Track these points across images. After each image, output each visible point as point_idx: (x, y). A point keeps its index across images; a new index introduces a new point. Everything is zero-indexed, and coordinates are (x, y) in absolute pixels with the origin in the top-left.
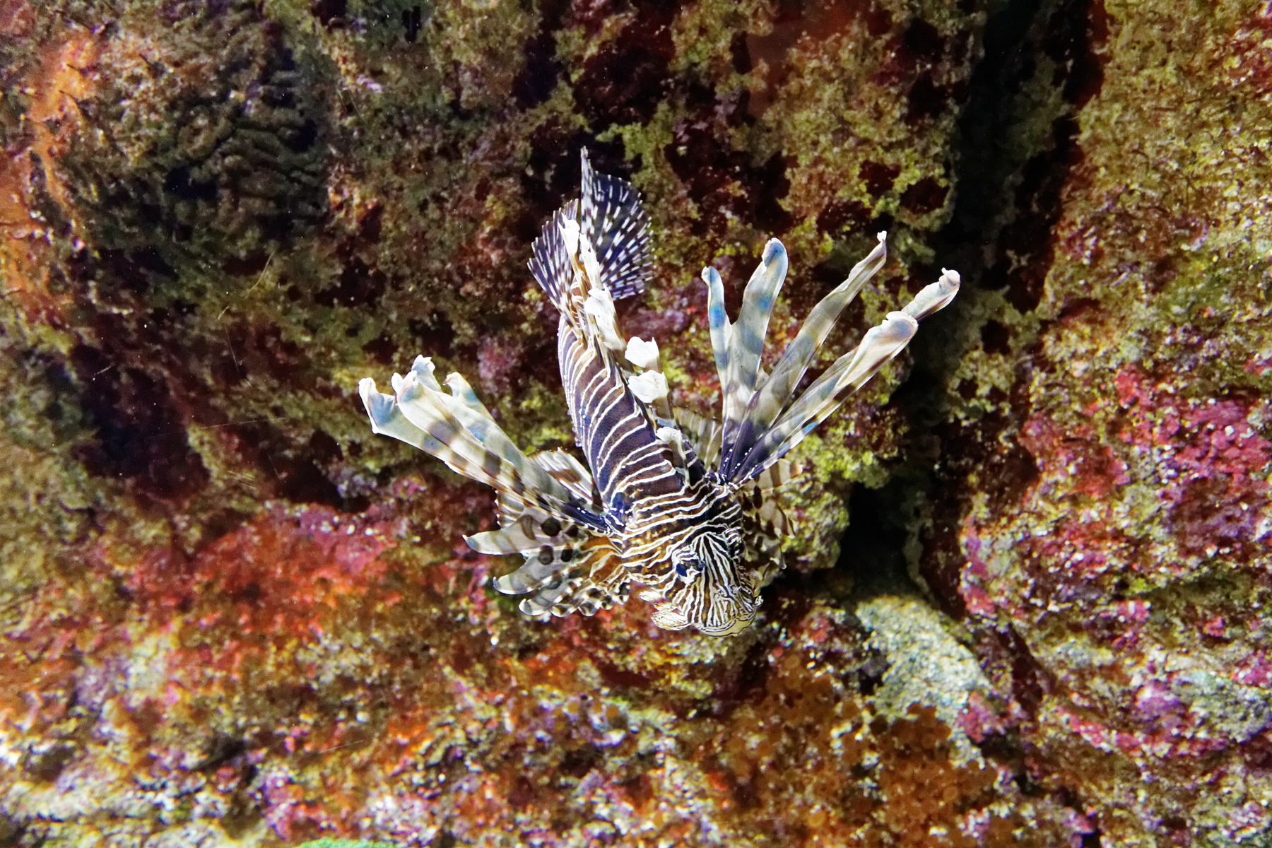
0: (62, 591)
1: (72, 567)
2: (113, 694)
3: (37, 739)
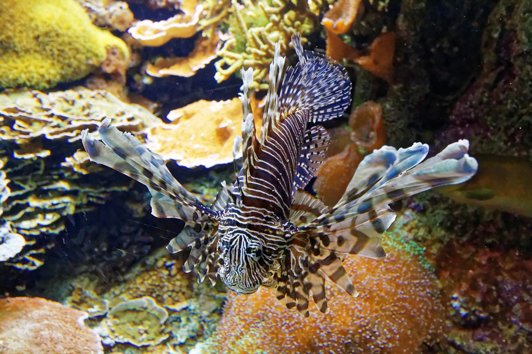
0: (500, 231)
2: (521, 300)
3: (481, 309)
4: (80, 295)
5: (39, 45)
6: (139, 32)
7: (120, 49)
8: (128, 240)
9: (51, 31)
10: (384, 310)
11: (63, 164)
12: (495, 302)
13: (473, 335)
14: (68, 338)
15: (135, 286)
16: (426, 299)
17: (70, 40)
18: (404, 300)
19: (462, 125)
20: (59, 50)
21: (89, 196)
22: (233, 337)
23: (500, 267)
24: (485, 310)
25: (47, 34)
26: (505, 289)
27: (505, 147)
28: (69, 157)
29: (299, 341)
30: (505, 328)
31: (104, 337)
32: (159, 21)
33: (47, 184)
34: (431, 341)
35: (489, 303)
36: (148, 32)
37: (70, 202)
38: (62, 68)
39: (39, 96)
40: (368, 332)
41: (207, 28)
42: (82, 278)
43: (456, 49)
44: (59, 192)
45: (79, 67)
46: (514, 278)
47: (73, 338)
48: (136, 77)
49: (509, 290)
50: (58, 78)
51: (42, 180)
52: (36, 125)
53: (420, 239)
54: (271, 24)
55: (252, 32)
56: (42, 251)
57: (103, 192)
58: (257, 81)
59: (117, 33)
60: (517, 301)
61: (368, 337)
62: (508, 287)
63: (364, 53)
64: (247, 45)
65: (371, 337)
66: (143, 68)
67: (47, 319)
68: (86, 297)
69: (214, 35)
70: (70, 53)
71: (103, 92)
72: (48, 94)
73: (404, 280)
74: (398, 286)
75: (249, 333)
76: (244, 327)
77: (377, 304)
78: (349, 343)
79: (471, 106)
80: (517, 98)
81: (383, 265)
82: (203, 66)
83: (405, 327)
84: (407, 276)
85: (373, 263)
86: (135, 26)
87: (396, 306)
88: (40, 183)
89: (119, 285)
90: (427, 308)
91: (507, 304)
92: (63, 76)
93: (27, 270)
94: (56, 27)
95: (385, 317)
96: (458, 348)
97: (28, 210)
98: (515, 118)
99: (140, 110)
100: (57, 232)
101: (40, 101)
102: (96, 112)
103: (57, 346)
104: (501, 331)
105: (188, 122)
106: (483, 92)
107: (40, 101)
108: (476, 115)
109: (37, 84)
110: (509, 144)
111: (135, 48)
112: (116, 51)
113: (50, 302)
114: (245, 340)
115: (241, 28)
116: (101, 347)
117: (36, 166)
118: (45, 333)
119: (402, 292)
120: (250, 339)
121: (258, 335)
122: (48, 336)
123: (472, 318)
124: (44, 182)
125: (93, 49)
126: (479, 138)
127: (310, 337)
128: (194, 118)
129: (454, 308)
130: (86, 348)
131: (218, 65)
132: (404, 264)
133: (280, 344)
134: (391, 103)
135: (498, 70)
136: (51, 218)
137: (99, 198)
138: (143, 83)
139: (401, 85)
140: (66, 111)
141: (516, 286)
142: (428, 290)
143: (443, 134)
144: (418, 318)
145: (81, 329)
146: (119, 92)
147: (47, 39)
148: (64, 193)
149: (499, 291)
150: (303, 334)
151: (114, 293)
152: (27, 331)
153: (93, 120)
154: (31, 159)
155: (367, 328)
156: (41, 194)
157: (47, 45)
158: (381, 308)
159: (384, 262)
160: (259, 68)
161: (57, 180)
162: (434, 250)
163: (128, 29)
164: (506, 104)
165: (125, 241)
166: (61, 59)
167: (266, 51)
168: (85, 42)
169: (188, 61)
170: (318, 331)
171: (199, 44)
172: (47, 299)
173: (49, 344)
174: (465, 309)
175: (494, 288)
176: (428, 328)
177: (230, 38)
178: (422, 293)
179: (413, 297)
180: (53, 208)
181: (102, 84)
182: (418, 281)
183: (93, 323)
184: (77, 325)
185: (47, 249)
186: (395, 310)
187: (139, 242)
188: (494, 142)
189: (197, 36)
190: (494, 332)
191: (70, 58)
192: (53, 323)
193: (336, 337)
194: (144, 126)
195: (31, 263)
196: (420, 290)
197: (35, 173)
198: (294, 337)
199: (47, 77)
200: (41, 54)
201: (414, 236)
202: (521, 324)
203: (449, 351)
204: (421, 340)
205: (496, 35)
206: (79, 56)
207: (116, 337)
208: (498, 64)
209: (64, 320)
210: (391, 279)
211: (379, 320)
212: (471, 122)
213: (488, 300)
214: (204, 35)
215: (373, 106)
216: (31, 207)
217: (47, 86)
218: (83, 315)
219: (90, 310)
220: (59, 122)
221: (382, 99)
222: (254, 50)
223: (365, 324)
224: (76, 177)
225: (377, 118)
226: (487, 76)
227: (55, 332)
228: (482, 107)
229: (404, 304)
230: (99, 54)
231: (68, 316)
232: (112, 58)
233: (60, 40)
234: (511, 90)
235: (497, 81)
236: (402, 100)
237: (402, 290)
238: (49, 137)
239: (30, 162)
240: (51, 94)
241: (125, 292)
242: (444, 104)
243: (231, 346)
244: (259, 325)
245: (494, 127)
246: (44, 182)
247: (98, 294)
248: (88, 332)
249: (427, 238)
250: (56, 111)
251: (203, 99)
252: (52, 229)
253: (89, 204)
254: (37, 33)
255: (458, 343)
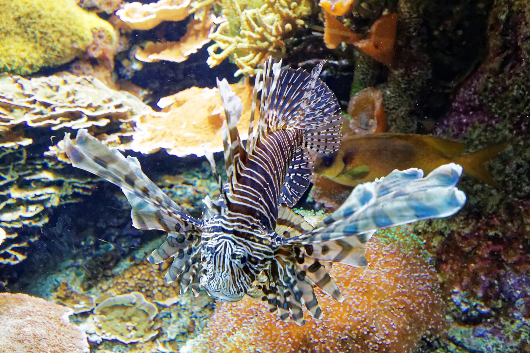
0: (504, 223)
1: (516, 211)
3: (483, 304)
4: (65, 290)
5: (20, 27)
6: (128, 15)
7: (108, 32)
8: (117, 233)
9: (33, 13)
10: (382, 305)
11: (46, 153)
12: (497, 297)
13: (474, 331)
14: (52, 335)
15: (123, 281)
16: (425, 293)
17: (54, 21)
18: (404, 294)
19: (466, 113)
20: (41, 33)
21: (74, 187)
22: (224, 334)
23: (503, 261)
24: (487, 306)
25: (28, 15)
26: (508, 283)
27: (510, 135)
28: (52, 145)
29: (294, 337)
30: (507, 323)
31: (90, 334)
32: (148, 4)
33: (30, 175)
34: (430, 336)
35: (491, 298)
36: (136, 15)
37: (54, 193)
38: (45, 52)
39: (19, 81)
40: (365, 328)
41: (199, 10)
42: (68, 272)
43: (460, 32)
44: (43, 182)
45: (63, 51)
46: (517, 271)
47: (57, 335)
48: (125, 63)
49: (512, 284)
50: (41, 63)
51: (24, 170)
52: (17, 112)
53: (420, 231)
54: (266, 5)
55: (246, 14)
56: (24, 244)
57: (89, 183)
58: (251, 66)
59: (104, 16)
60: (520, 296)
61: (366, 333)
62: (511, 282)
63: (365, 36)
64: (241, 28)
65: (368, 333)
66: (132, 53)
67: (30, 315)
68: (72, 292)
69: (206, 18)
70: (54, 37)
71: (89, 78)
72: (30, 79)
73: (404, 273)
74: (397, 280)
75: (242, 329)
76: (236, 322)
77: (375, 299)
78: (346, 339)
79: (475, 93)
80: (523, 84)
81: (382, 258)
82: (195, 51)
83: (404, 323)
84: (407, 269)
85: (371, 256)
86: (123, 8)
87: (395, 300)
88: (21, 174)
89: (107, 280)
90: (427, 303)
91: (510, 299)
92: (46, 61)
93: (8, 265)
94: (38, 8)
95: (383, 312)
96: (458, 344)
97: (10, 201)
98: (521, 105)
99: (129, 97)
100: (40, 224)
101: (22, 87)
102: (81, 98)
103: (40, 343)
104: (503, 326)
105: (179, 109)
106: (489, 78)
107: (22, 87)
108: (481, 101)
109: (19, 68)
110: (515, 132)
111: (123, 31)
112: (102, 34)
113: (33, 298)
114: (237, 336)
115: (235, 10)
116: (87, 345)
117: (18, 155)
118: (28, 330)
119: (402, 286)
120: (243, 336)
121: (251, 331)
122: (31, 333)
123: (473, 312)
124: (27, 172)
125: (78, 32)
126: (483, 126)
127: (305, 333)
128: (185, 105)
129: (455, 303)
130: (71, 345)
131: (211, 50)
132: (404, 257)
133: (274, 341)
134: (392, 89)
135: (505, 54)
136: (34, 210)
137: (84, 189)
138: (132, 69)
139: (402, 71)
140: (48, 97)
141: (519, 281)
142: (428, 284)
143: (445, 122)
144: (417, 313)
145: (65, 326)
146: (106, 78)
147: (28, 21)
148: (49, 184)
149: (502, 285)
150: (298, 330)
151: (101, 288)
152: (9, 327)
153: (78, 106)
154: (12, 148)
155: (365, 323)
156: (23, 184)
157: (29, 27)
158: (379, 303)
159: (383, 255)
160: (253, 53)
161: (40, 170)
162: (435, 242)
163: (115, 11)
164: (513, 90)
165: (112, 234)
166: (44, 42)
167: (261, 34)
168: (70, 24)
169: (179, 46)
170: (314, 326)
171: (192, 27)
172: (31, 294)
173: (32, 340)
174: (466, 303)
175: (496, 282)
176: (427, 323)
177: (224, 21)
178: (422, 287)
179: (413, 291)
180: (36, 199)
181: (88, 69)
182: (417, 274)
183: (80, 319)
184: (61, 322)
185: (30, 243)
186: (394, 305)
187: (127, 235)
188: (499, 130)
189: (189, 19)
190: (496, 328)
191: (53, 41)
192: (36, 319)
193: (332, 333)
194: (132, 114)
195: (13, 257)
196: (420, 284)
197: (16, 163)
198: (288, 333)
199: (29, 62)
200: (23, 37)
201: (414, 229)
202: (523, 319)
203: (448, 347)
204: (420, 335)
205: (503, 17)
206: (62, 39)
207: (104, 334)
208: (504, 47)
209: (48, 317)
210: (390, 272)
211: (377, 315)
212: (475, 109)
213: (491, 294)
214: (196, 18)
215: (374, 92)
216: (13, 199)
217: (30, 71)
218: (68, 311)
219: (76, 306)
220: (42, 108)
221: (382, 85)
222: (248, 33)
223: (363, 319)
224: (60, 166)
225: (378, 104)
226: (491, 61)
227: (38, 328)
228: (487, 93)
229: (403, 298)
230: (85, 38)
231: (52, 312)
232: (99, 41)
233: (43, 22)
234: (518, 75)
235: (503, 65)
236: (403, 86)
237: (401, 284)
238: (30, 124)
239: (10, 151)
240: (33, 79)
241: (113, 287)
242: (447, 91)
243: (222, 343)
244: (252, 321)
245: (500, 115)
246: (27, 172)
247: (84, 290)
248: (73, 329)
249: (427, 230)
250: (39, 97)
251: (196, 86)
252: (35, 222)
253: (75, 195)
254: (17, 14)
255: (459, 339)
